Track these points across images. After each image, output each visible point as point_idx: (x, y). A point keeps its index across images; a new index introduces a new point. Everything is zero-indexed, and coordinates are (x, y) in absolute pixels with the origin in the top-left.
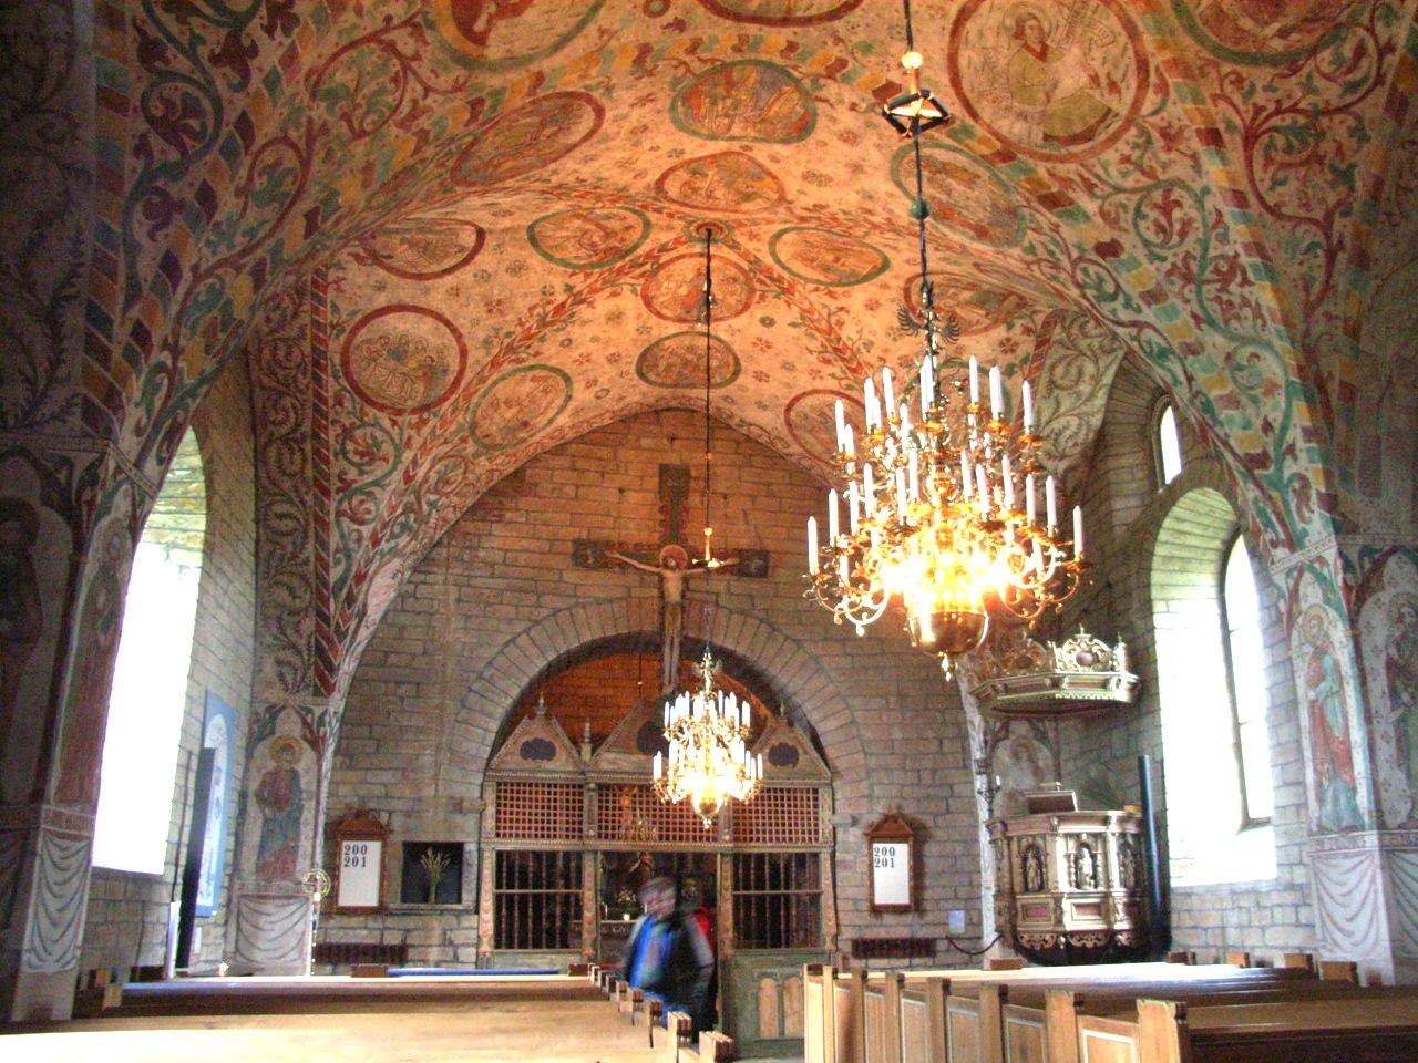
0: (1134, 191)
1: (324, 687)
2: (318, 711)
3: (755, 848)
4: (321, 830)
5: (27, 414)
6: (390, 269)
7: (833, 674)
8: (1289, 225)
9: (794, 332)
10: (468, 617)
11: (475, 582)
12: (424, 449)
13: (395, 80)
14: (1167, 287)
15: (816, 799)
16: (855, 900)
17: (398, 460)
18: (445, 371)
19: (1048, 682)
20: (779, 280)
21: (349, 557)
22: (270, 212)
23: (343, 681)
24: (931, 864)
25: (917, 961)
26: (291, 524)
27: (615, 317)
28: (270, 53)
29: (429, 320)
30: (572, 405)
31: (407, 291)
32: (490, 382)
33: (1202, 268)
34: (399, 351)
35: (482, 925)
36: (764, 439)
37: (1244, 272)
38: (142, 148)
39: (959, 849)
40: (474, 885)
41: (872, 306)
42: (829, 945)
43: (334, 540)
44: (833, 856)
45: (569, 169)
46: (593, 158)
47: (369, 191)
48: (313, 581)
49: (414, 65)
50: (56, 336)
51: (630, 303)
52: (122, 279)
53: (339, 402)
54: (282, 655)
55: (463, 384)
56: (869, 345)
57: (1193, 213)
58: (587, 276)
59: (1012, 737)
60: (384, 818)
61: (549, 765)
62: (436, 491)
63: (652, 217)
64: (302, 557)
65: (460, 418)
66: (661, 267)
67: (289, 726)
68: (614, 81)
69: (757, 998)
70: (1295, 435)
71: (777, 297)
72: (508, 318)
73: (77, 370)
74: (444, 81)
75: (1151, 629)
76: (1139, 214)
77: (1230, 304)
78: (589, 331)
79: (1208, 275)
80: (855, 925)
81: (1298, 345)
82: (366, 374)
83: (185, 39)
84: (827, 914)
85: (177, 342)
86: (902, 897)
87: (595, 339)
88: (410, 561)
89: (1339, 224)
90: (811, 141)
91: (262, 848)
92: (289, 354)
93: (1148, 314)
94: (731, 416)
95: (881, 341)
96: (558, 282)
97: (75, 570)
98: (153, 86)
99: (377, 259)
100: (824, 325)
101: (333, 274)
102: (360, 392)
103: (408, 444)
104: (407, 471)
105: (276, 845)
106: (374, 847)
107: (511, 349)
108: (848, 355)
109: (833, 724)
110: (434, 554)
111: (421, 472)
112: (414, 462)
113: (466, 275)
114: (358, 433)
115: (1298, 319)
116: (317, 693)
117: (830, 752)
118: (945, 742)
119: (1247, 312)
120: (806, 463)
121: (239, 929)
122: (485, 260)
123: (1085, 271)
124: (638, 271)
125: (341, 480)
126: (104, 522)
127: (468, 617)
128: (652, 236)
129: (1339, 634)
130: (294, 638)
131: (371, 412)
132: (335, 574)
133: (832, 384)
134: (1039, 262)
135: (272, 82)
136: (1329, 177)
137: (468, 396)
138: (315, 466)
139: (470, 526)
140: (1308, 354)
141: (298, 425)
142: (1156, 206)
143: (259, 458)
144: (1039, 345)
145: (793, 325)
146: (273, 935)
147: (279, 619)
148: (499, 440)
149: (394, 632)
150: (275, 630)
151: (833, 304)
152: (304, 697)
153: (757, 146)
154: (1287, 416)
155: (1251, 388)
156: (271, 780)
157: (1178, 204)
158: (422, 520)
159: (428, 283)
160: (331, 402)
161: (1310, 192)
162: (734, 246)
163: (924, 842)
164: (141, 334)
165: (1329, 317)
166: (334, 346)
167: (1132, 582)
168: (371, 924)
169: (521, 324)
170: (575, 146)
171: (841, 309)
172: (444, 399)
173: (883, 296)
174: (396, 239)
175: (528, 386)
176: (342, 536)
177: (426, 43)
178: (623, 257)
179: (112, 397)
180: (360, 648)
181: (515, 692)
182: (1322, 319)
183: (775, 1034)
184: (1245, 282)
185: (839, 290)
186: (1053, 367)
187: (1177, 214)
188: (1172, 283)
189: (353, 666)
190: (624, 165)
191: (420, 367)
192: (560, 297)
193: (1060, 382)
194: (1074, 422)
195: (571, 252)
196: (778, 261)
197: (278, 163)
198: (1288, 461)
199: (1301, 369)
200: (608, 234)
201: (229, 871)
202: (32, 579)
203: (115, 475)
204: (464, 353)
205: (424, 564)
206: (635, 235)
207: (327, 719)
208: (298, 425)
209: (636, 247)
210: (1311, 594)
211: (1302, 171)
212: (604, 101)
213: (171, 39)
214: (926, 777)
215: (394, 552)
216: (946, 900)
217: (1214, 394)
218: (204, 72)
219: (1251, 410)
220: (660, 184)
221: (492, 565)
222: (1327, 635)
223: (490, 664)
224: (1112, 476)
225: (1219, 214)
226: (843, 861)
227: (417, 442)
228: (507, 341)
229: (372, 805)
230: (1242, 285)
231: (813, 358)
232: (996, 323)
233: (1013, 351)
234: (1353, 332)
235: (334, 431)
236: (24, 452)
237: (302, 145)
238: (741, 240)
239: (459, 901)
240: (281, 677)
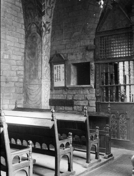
207: (43, 24)
239: (89, 84)
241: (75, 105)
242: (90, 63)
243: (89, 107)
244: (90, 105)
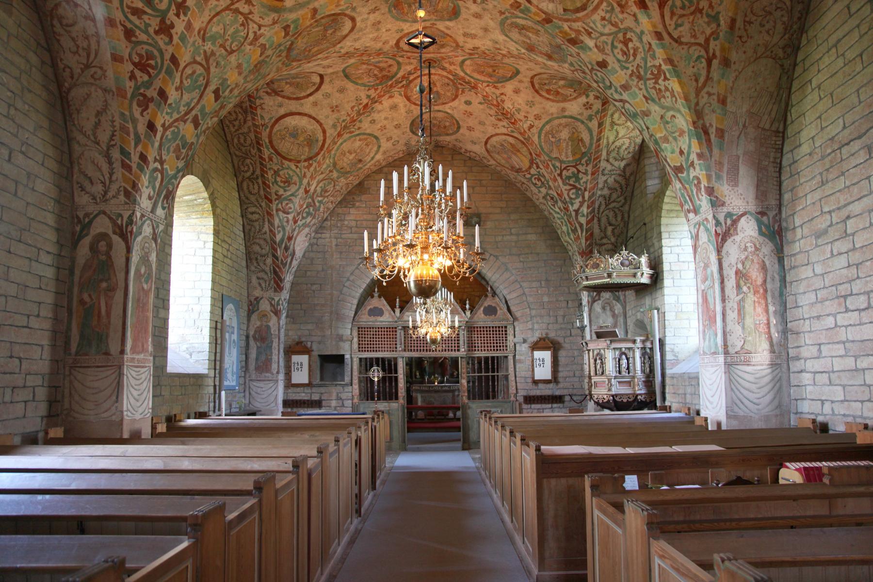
0: (609, 35)
1: (279, 288)
2: (276, 299)
3: (477, 354)
4: (282, 351)
5: (104, 196)
6: (283, 97)
7: (514, 272)
8: (686, 47)
9: (481, 107)
10: (341, 253)
11: (343, 236)
12: (312, 178)
13: (243, 25)
14: (631, 83)
16: (526, 378)
17: (301, 184)
18: (317, 141)
19: (606, 275)
20: (468, 83)
21: (284, 229)
22: (196, 94)
23: (287, 285)
24: (562, 360)
25: (555, 405)
26: (257, 216)
27: (394, 107)
28: (180, 26)
29: (306, 118)
30: (381, 150)
31: (293, 106)
32: (339, 143)
33: (646, 73)
34: (294, 134)
36: (477, 159)
37: (665, 74)
38: (132, 77)
39: (576, 353)
40: (350, 373)
41: (517, 91)
42: (512, 398)
43: (277, 222)
44: (514, 356)
45: (347, 45)
46: (358, 39)
47: (243, 75)
48: (269, 241)
49: (250, 16)
50: (110, 163)
51: (399, 100)
52: (132, 136)
53: (271, 159)
54: (259, 275)
55: (326, 146)
56: (518, 110)
57: (638, 44)
58: (376, 90)
59: (602, 299)
60: (309, 344)
61: (381, 319)
62: (321, 196)
63: (400, 60)
64: (264, 230)
65: (327, 161)
66: (411, 82)
67: (265, 306)
68: (354, 5)
70: (693, 157)
71: (470, 90)
72: (343, 113)
73: (120, 176)
74: (268, 20)
75: (661, 247)
76: (613, 47)
77: (660, 89)
78: (383, 115)
79: (649, 76)
80: (526, 389)
81: (692, 111)
82: (281, 146)
83: (143, 26)
84: (512, 384)
85: (161, 158)
87: (386, 119)
88: (313, 229)
89: (712, 44)
90: (461, 18)
91: (257, 359)
92: (245, 140)
93: (625, 96)
94: (461, 148)
95: (524, 107)
96: (363, 95)
97: (128, 260)
98: (133, 49)
99: (276, 93)
100: (495, 103)
101: (258, 102)
102: (279, 154)
103: (305, 176)
104: (305, 189)
105: (263, 358)
106: (304, 359)
107: (345, 127)
108: (509, 116)
109: (514, 295)
110: (324, 225)
111: (312, 188)
112: (309, 184)
113: (318, 96)
114: (281, 173)
115: (692, 96)
116: (275, 291)
117: (512, 308)
119: (668, 94)
120: (499, 169)
121: (250, 394)
122: (326, 88)
123: (596, 74)
124: (400, 85)
125: (276, 195)
126: (139, 239)
127: (341, 253)
128: (403, 68)
129: (713, 258)
130: (264, 267)
131: (286, 163)
132: (278, 238)
133: (504, 131)
134: (577, 70)
135: (183, 38)
136: (706, 20)
137: (329, 151)
138: (264, 189)
139: (340, 211)
140: (698, 114)
141: (254, 172)
142: (621, 42)
143: (240, 188)
144: (604, 104)
145: (480, 103)
146: (264, 396)
147: (257, 259)
148: (348, 169)
149: (309, 262)
150: (255, 264)
151: (498, 92)
152: (271, 293)
153: (438, 23)
154: (690, 147)
155: (673, 133)
156: (258, 330)
157: (631, 40)
158: (317, 210)
159: (302, 101)
160: (267, 160)
161: (696, 28)
162: (444, 69)
163: (559, 349)
164: (143, 158)
165: (709, 94)
166: (265, 135)
167: (654, 222)
168: (306, 391)
169: (349, 115)
170: (346, 36)
171: (502, 94)
172: (318, 154)
173: (522, 86)
174: (283, 83)
175: (358, 144)
176: (280, 220)
177: (253, 6)
178: (391, 79)
179: (134, 186)
180: (294, 270)
181: (364, 286)
182: (706, 96)
184: (666, 79)
185: (499, 85)
186: (612, 115)
187: (630, 45)
188: (633, 80)
189: (291, 278)
190: (375, 39)
191: (305, 139)
192: (365, 101)
193: (617, 122)
194: (627, 141)
195: (366, 80)
196: (466, 74)
197: (194, 72)
198: (692, 170)
199: (694, 123)
200: (382, 70)
201: (244, 369)
202: (112, 265)
203: (141, 218)
204: (324, 132)
205: (320, 229)
206: (394, 69)
208: (254, 172)
209: (396, 74)
210: (703, 237)
211: (691, 18)
212: (353, 14)
213: (136, 26)
214: (560, 319)
215: (305, 225)
217: (658, 135)
218: (153, 39)
219: (674, 144)
220: (397, 44)
221: (351, 228)
222: (709, 258)
223: (352, 274)
224: (647, 169)
225: (650, 44)
227: (308, 175)
228: (344, 124)
229: (303, 339)
230: (664, 80)
231: (493, 118)
232: (580, 95)
233: (591, 108)
234: (723, 102)
235: (271, 173)
236: (104, 213)
237: (204, 63)
238: (447, 65)
240: (260, 284)
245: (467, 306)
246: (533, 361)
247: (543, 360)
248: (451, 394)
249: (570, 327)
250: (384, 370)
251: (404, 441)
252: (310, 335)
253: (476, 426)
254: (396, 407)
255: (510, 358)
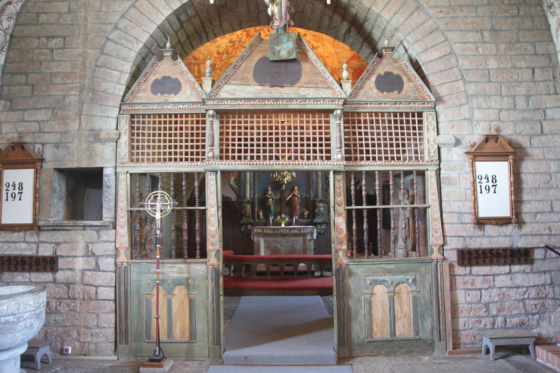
3: (366, 166)
15: (420, 122)
24: (528, 180)
35: (119, 238)
40: (112, 204)
42: (436, 255)
44: (438, 172)
69: (370, 303)
86: (505, 211)
106: (25, 176)
118: (536, 70)
168: (29, 239)
183: (387, 336)
214: (521, 103)
216: (543, 213)
223: (123, 16)
226: (448, 178)
229: (28, 139)
239: (100, 217)
241: (62, 269)
242: (104, 169)
243: (100, 273)
244: (101, 268)
245: (345, 74)
246: (474, 182)
247: (494, 179)
248: (301, 239)
249: (540, 117)
250: (177, 196)
251: (217, 342)
252: (41, 131)
253: (363, 311)
254: (202, 272)
255: (431, 177)
